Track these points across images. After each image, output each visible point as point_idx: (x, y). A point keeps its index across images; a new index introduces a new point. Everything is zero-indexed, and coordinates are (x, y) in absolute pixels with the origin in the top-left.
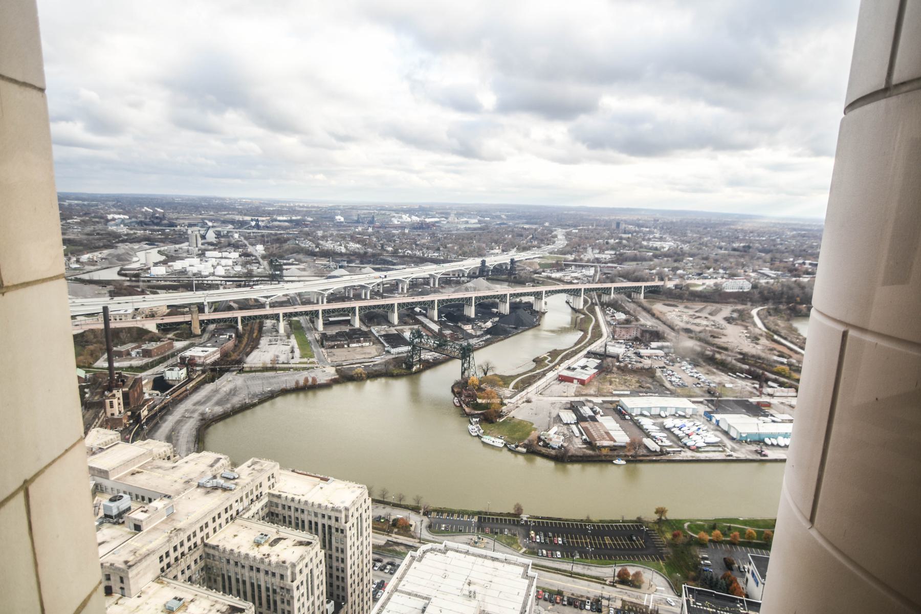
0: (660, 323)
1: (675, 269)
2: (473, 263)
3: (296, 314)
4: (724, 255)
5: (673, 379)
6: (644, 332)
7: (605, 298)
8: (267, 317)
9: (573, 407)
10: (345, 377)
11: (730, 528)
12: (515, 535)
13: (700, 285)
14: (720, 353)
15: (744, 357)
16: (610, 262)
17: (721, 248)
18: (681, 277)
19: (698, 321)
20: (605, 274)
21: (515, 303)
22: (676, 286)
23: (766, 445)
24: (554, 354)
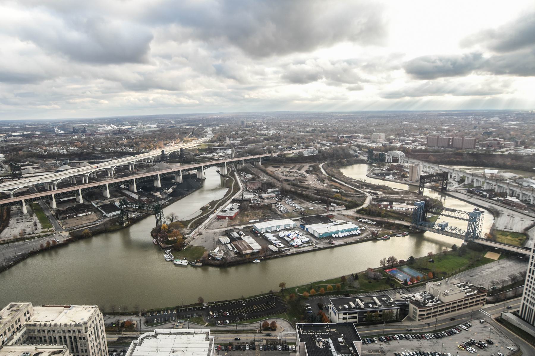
0: (271, 177)
1: (277, 146)
2: (155, 153)
3: (35, 199)
4: (302, 136)
5: (282, 209)
6: (263, 184)
7: (239, 167)
8: (12, 204)
9: (227, 234)
10: (77, 237)
11: (319, 287)
12: (201, 316)
13: (291, 153)
14: (305, 191)
15: (318, 192)
16: (240, 145)
17: (300, 132)
18: (281, 150)
19: (292, 174)
20: (238, 152)
21: (186, 175)
22: (278, 155)
23: (333, 238)
24: (213, 203)
